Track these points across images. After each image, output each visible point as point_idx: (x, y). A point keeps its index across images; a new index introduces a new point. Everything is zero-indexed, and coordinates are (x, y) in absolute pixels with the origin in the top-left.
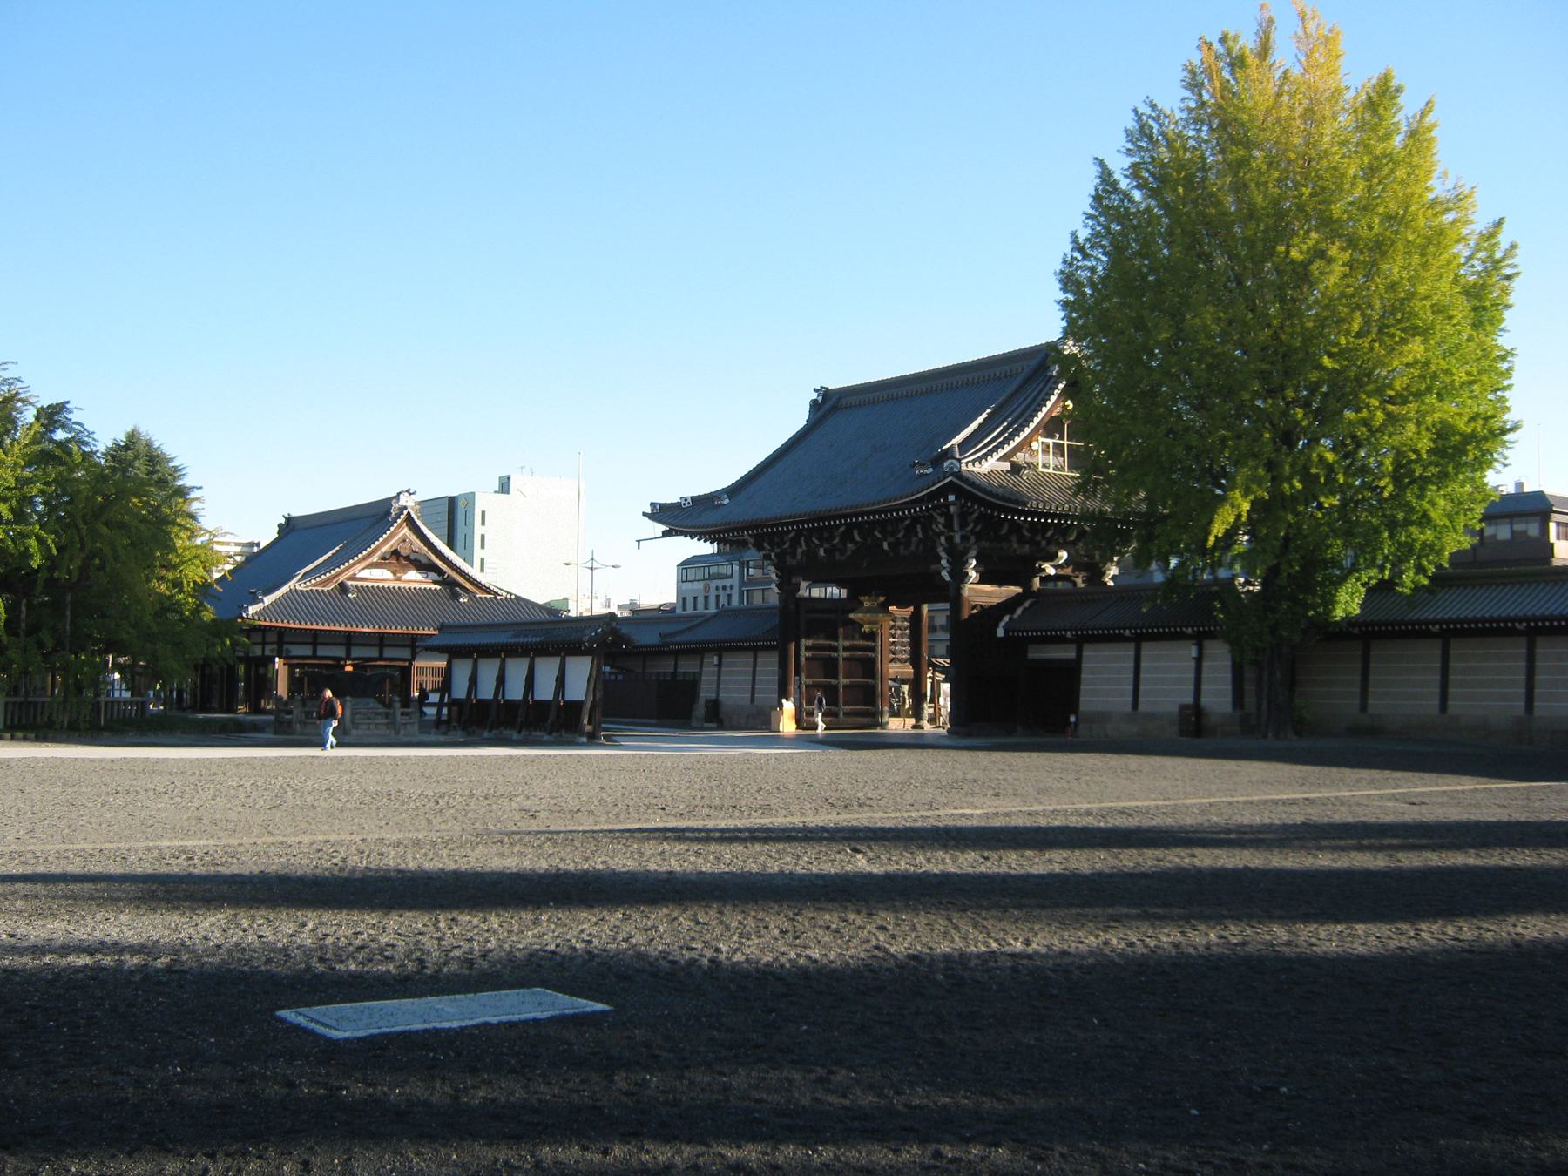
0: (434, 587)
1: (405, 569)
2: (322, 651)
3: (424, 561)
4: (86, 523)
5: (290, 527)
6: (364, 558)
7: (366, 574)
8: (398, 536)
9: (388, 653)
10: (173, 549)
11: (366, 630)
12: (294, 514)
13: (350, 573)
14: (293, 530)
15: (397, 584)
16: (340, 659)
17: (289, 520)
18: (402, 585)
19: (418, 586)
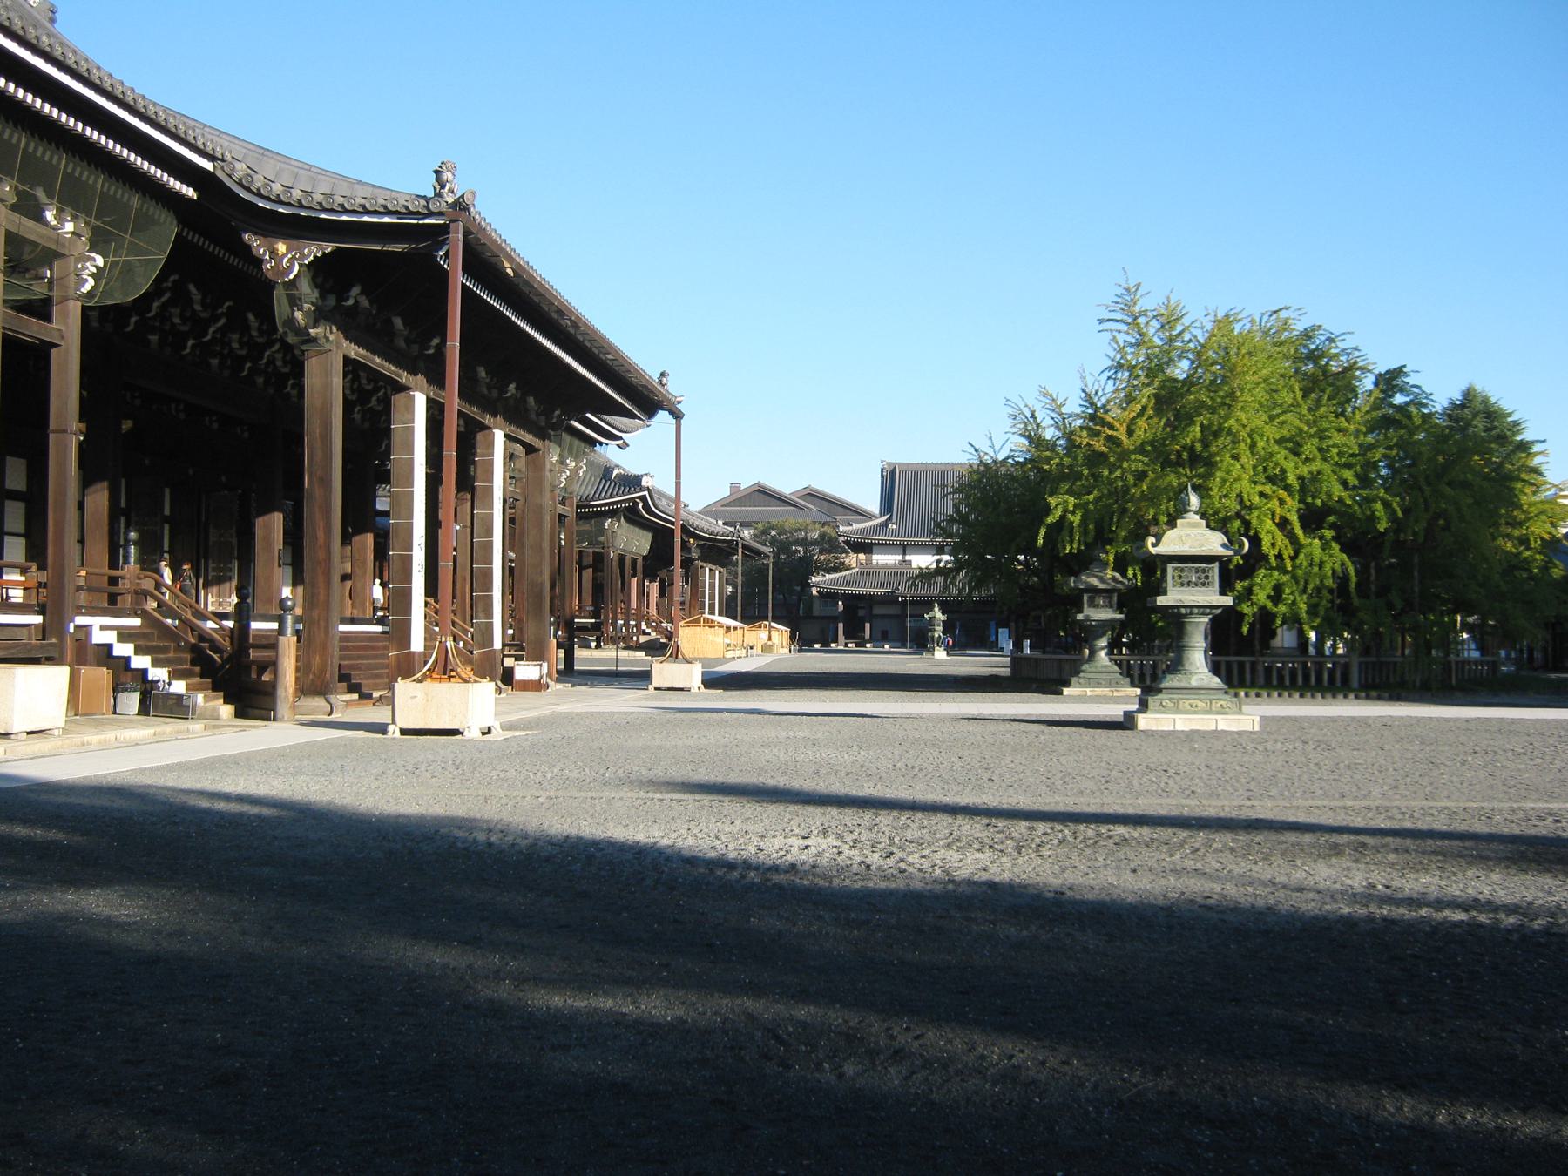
4: (1429, 484)
10: (1519, 506)
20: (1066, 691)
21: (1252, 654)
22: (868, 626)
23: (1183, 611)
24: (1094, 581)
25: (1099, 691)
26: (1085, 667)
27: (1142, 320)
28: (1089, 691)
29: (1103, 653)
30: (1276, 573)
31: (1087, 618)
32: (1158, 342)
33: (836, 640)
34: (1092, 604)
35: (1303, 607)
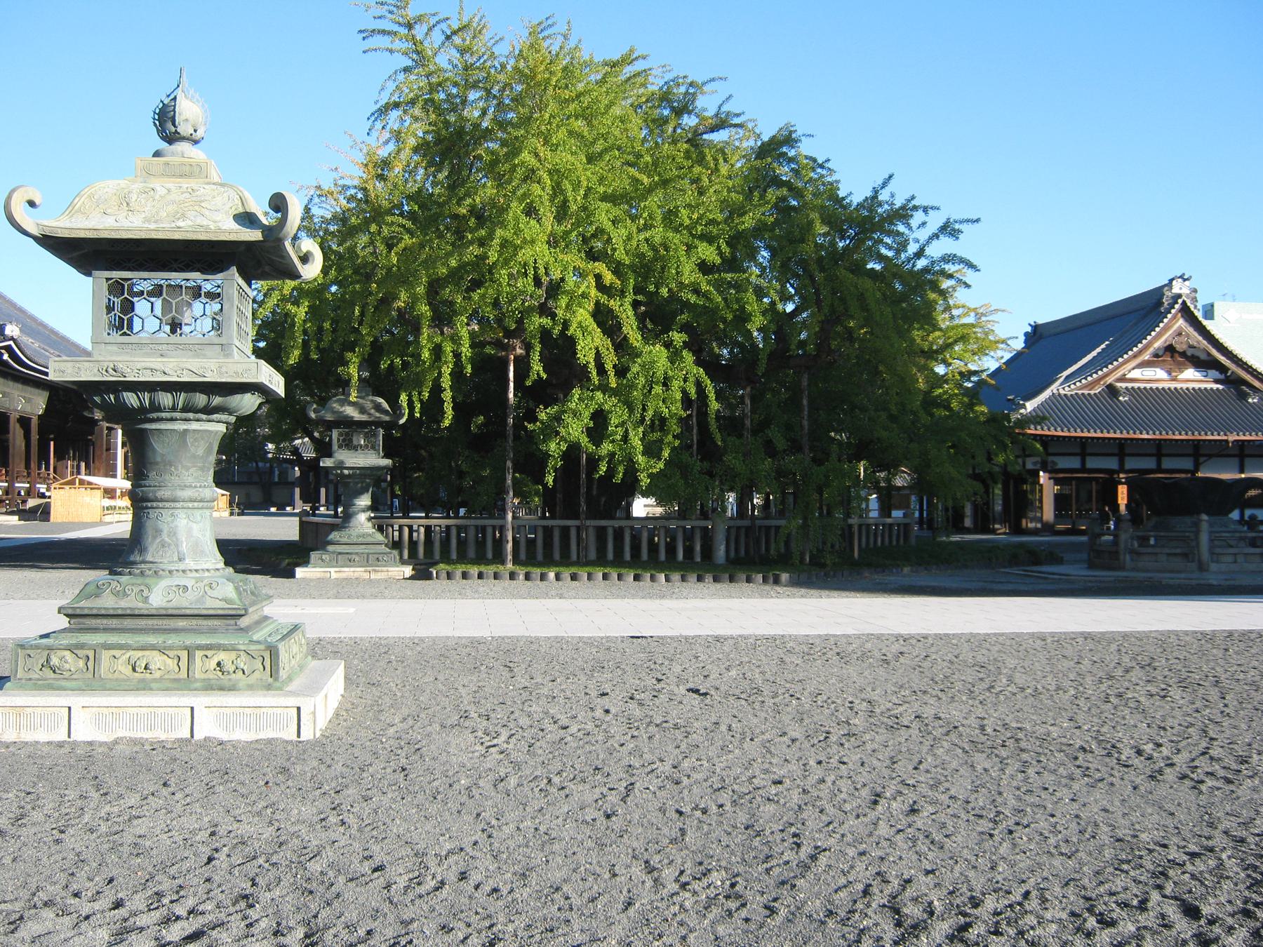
0: (1215, 386)
1: (1181, 368)
2: (1092, 463)
3: (1203, 357)
4: (822, 270)
5: (1037, 335)
6: (1135, 356)
7: (1136, 374)
8: (1172, 329)
9: (1167, 463)
10: (935, 327)
11: (1145, 436)
12: (1040, 322)
13: (1119, 374)
14: (1041, 337)
15: (1173, 385)
16: (1111, 472)
17: (1036, 328)
18: (1179, 386)
19: (1197, 386)
20: (300, 572)
21: (577, 517)
22: (323, 491)
23: (131, 399)
24: (351, 411)
25: (348, 572)
26: (334, 536)
27: (419, 31)
28: (334, 573)
29: (362, 517)
30: (599, 395)
31: (340, 465)
32: (442, 60)
33: (292, 504)
34: (348, 444)
35: (636, 442)
